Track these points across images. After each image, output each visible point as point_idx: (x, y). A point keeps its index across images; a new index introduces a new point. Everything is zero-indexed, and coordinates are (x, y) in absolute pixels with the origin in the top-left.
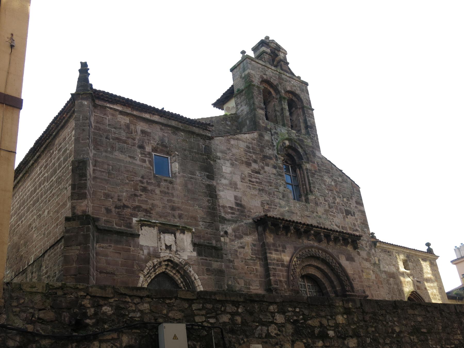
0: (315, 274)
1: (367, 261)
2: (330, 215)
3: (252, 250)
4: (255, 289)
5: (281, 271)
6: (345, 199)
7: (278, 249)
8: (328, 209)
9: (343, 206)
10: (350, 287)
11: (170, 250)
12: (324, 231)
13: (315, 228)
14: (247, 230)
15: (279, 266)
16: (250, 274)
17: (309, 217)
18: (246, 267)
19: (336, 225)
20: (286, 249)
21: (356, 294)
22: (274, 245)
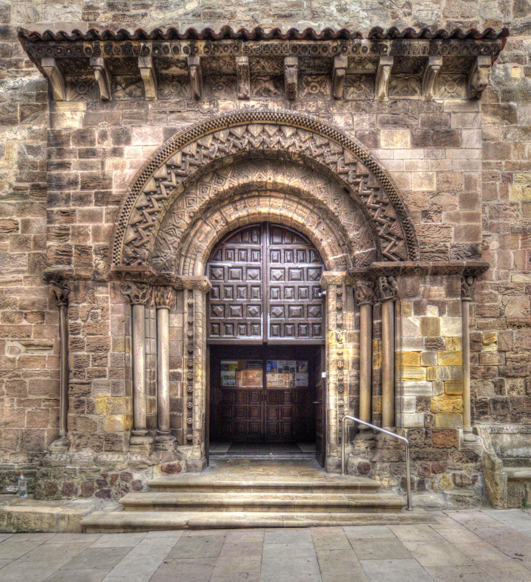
3: (20, 167)
5: (92, 217)
7: (97, 146)
10: (401, 244)
13: (251, 44)
20: (128, 141)
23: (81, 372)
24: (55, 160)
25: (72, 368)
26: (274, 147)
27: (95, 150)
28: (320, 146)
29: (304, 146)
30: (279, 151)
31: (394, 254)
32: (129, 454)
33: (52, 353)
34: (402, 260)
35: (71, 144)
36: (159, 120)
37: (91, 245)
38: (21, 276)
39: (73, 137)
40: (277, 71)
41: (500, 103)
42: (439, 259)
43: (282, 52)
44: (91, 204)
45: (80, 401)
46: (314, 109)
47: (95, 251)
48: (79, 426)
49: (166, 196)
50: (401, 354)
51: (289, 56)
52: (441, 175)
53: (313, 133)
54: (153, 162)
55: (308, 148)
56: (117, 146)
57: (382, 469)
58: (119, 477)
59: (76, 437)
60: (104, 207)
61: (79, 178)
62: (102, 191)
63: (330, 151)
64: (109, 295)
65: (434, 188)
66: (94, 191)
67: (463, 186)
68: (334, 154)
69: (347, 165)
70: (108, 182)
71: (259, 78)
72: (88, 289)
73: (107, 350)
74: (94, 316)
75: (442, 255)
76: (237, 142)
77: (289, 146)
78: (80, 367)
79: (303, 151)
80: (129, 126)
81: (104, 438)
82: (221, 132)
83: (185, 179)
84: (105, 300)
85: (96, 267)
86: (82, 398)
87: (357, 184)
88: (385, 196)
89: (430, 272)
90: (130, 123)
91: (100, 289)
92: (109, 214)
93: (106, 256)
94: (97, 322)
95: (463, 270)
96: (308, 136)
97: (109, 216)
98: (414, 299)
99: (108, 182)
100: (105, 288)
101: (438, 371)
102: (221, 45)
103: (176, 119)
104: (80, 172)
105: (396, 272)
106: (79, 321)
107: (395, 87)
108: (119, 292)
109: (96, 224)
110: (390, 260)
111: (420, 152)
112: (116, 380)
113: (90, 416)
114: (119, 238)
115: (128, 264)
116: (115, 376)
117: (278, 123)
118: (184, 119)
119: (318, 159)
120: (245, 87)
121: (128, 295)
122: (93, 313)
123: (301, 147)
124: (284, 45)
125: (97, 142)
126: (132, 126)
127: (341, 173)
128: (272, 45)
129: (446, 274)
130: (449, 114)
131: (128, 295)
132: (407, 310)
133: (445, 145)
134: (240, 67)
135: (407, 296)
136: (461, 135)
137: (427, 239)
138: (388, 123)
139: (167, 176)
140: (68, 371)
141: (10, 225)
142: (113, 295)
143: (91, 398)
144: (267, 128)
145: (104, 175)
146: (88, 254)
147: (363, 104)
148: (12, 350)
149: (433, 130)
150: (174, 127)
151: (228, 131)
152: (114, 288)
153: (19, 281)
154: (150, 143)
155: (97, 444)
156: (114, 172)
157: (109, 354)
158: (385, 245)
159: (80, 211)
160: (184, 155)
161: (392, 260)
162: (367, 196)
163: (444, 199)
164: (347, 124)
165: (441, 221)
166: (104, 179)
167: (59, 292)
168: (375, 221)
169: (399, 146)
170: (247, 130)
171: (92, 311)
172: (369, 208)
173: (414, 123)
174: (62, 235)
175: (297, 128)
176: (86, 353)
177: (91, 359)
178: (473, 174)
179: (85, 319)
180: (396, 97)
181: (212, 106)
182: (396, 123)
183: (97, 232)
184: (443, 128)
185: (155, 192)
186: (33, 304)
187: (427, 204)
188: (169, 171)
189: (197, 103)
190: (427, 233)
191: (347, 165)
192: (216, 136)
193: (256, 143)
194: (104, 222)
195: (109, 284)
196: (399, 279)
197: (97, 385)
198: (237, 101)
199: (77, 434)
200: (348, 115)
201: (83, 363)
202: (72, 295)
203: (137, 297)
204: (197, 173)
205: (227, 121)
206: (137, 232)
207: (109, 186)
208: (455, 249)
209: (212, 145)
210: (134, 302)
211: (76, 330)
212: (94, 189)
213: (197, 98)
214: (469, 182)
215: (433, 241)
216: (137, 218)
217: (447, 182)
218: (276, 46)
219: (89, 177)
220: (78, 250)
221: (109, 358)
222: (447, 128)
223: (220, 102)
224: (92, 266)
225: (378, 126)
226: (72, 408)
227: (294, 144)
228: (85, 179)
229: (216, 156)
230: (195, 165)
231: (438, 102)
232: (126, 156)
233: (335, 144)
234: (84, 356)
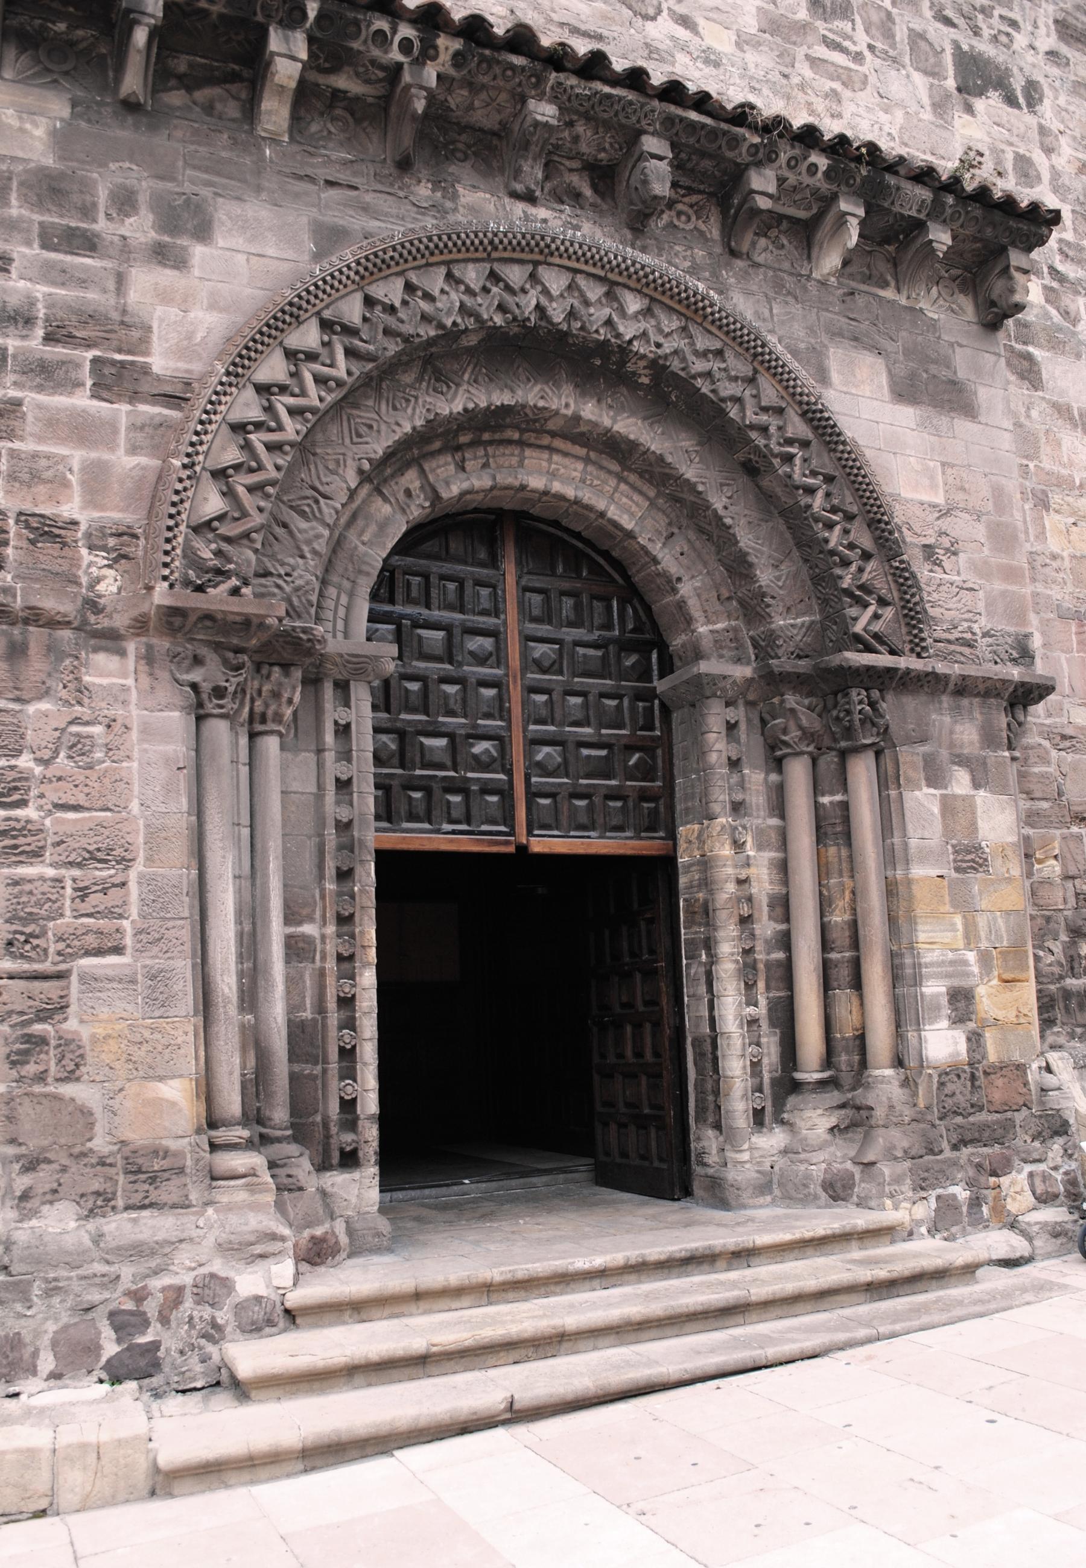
0: (587, 496)
2: (814, 62)
9: (948, 22)
12: (669, 121)
20: (203, 232)
21: (941, 668)
23: (32, 935)
26: (597, 331)
27: (97, 235)
28: (704, 354)
29: (668, 347)
30: (606, 342)
31: (876, 636)
32: (210, 1211)
34: (892, 652)
35: (14, 202)
36: (297, 196)
37: (76, 516)
39: (21, 184)
40: (602, 155)
41: (1013, 343)
42: (962, 659)
43: (638, 121)
44: (79, 392)
45: (28, 1038)
46: (688, 264)
47: (88, 535)
48: (27, 1126)
49: (317, 403)
50: (909, 882)
51: (653, 134)
52: (949, 471)
53: (687, 318)
54: (291, 304)
55: (676, 352)
56: (167, 239)
57: (898, 1180)
58: (188, 1292)
59: (17, 1167)
60: (124, 408)
61: (40, 306)
62: (118, 357)
63: (725, 370)
64: (130, 682)
65: (940, 499)
66: (90, 354)
67: (990, 503)
68: (735, 379)
69: (765, 409)
70: (136, 334)
71: (556, 158)
72: (60, 659)
73: (125, 862)
74: (79, 747)
75: (966, 651)
76: (509, 299)
77: (635, 337)
78: (31, 918)
79: (666, 357)
80: (206, 192)
81: (120, 1162)
82: (471, 266)
83: (370, 366)
84: (119, 696)
85: (91, 587)
86: (38, 1028)
87: (789, 459)
88: (849, 499)
89: (951, 686)
90: (208, 184)
91: (101, 659)
92: (142, 428)
93: (125, 557)
94: (91, 768)
95: (1011, 689)
96: (674, 323)
97: (140, 436)
99: (136, 334)
100: (116, 658)
102: (498, 62)
103: (345, 205)
104: (41, 290)
106: (25, 761)
108: (165, 675)
109: (94, 455)
110: (869, 649)
111: (907, 414)
112: (158, 963)
113: (68, 1090)
114: (181, 508)
115: (200, 589)
116: (155, 950)
117: (610, 276)
118: (365, 209)
119: (699, 382)
120: (533, 172)
121: (194, 686)
122: (78, 735)
123: (658, 345)
124: (648, 108)
125: (101, 216)
126: (216, 194)
127: (752, 427)
128: (620, 99)
129: (978, 695)
130: (952, 345)
131: (194, 686)
132: (911, 773)
133: (952, 410)
134: (536, 124)
136: (975, 393)
138: (841, 334)
139: (320, 350)
142: (145, 680)
143: (71, 1024)
144: (581, 281)
145: (124, 312)
146: (64, 544)
147: (789, 282)
149: (926, 371)
150: (341, 222)
151: (488, 266)
152: (148, 658)
154: (271, 251)
155: (96, 1186)
156: (160, 311)
157: (133, 875)
159: (40, 407)
162: (811, 491)
165: (959, 574)
166: (122, 323)
168: (833, 553)
169: (867, 390)
170: (533, 277)
171: (74, 729)
172: (817, 520)
175: (652, 299)
176: (51, 872)
177: (69, 891)
178: (1004, 481)
179: (46, 754)
180: (853, 284)
181: (439, 194)
184: (944, 374)
187: (930, 532)
188: (326, 338)
189: (401, 178)
190: (935, 595)
191: (765, 409)
192: (457, 273)
193: (557, 314)
194: (121, 451)
195: (131, 647)
196: (890, 696)
197: (88, 980)
198: (507, 200)
199: (18, 1158)
200: (761, 297)
201: (39, 904)
204: (399, 354)
205: (491, 242)
206: (229, 494)
207: (142, 345)
208: (990, 640)
209: (442, 291)
210: (210, 707)
212: (89, 347)
213: (404, 165)
215: (949, 615)
216: (232, 455)
217: (962, 489)
218: (631, 103)
219: (79, 312)
220: (28, 526)
221: (133, 887)
222: (950, 375)
223: (461, 190)
224: (79, 585)
225: (825, 338)
227: (644, 334)
228: (60, 314)
229: (454, 324)
230: (399, 334)
231: (930, 315)
232: (196, 272)
233: (738, 355)
234: (42, 879)
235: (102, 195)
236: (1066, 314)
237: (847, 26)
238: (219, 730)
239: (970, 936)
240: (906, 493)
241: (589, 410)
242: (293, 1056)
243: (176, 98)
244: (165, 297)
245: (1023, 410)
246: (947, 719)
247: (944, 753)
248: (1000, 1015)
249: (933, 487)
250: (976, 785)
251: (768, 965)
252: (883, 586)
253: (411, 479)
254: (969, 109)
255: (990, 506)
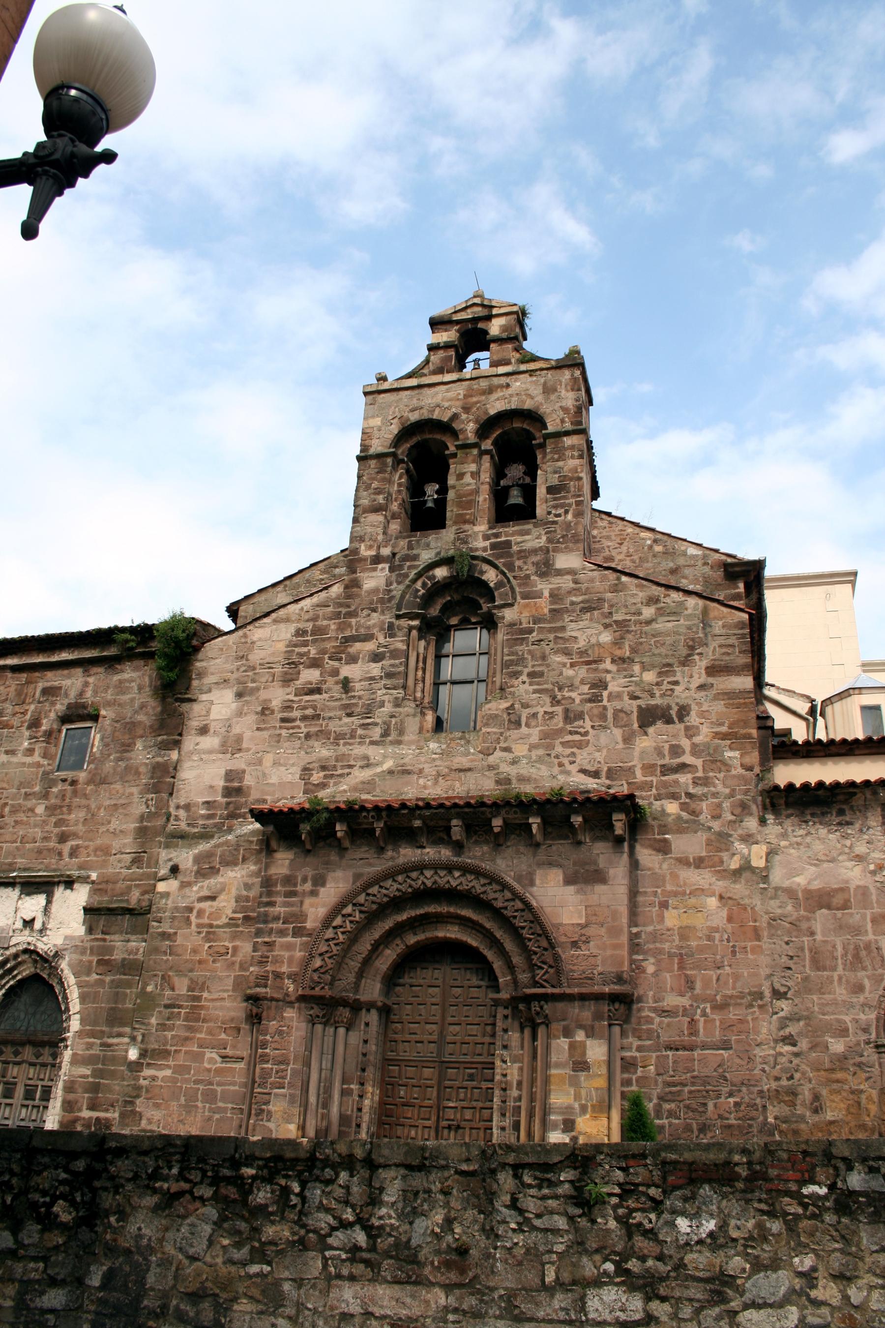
1: (698, 867)
4: (213, 1000)
5: (289, 947)
6: (650, 677)
7: (299, 888)
8: (561, 725)
9: (636, 698)
11: (32, 929)
14: (238, 851)
15: (286, 935)
16: (214, 961)
17: (470, 770)
18: (207, 945)
19: (583, 771)
20: (323, 884)
21: (568, 991)
22: (289, 880)
24: (265, 899)
25: (257, 1079)
28: (484, 885)
29: (471, 885)
31: (545, 981)
33: (242, 1065)
34: (553, 986)
38: (225, 995)
65: (583, 921)
73: (288, 1064)
74: (281, 1033)
87: (515, 917)
98: (563, 1023)
101: (583, 1092)
104: (283, 909)
105: (546, 997)
106: (268, 1037)
107: (550, 833)
110: (543, 986)
111: (571, 889)
118: (371, 865)
132: (556, 1033)
135: (558, 1020)
137: (575, 968)
140: (254, 1082)
141: (223, 950)
143: (270, 1107)
148: (211, 1060)
152: (299, 1009)
153: (223, 999)
158: (538, 972)
160: (368, 894)
161: (544, 987)
163: (591, 931)
164: (507, 866)
167: (255, 1010)
169: (552, 884)
170: (422, 873)
173: (566, 863)
174: (263, 961)
182: (551, 864)
183: (291, 960)
184: (592, 868)
185: (341, 927)
186: (232, 1020)
193: (429, 883)
197: (276, 1095)
202: (264, 1014)
203: (318, 1016)
206: (323, 960)
207: (305, 921)
211: (264, 1045)
214: (615, 914)
226: (253, 1116)
227: (461, 883)
235: (299, 878)
236: (693, 813)
237: (581, 723)
238: (319, 1028)
239: (577, 1097)
240: (566, 921)
241: (452, 910)
242: (340, 1125)
243: (321, 844)
244: (312, 905)
245: (657, 866)
246: (577, 1011)
247: (573, 1025)
248: (588, 1130)
249: (580, 917)
250: (588, 1036)
251: (514, 1107)
252: (550, 960)
253: (398, 941)
254: (646, 734)
255: (609, 919)
